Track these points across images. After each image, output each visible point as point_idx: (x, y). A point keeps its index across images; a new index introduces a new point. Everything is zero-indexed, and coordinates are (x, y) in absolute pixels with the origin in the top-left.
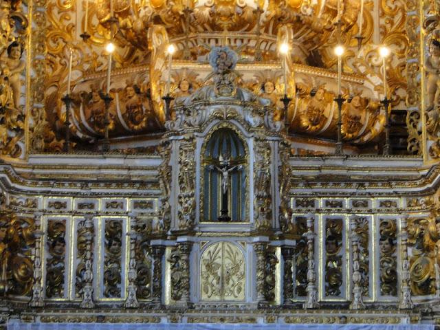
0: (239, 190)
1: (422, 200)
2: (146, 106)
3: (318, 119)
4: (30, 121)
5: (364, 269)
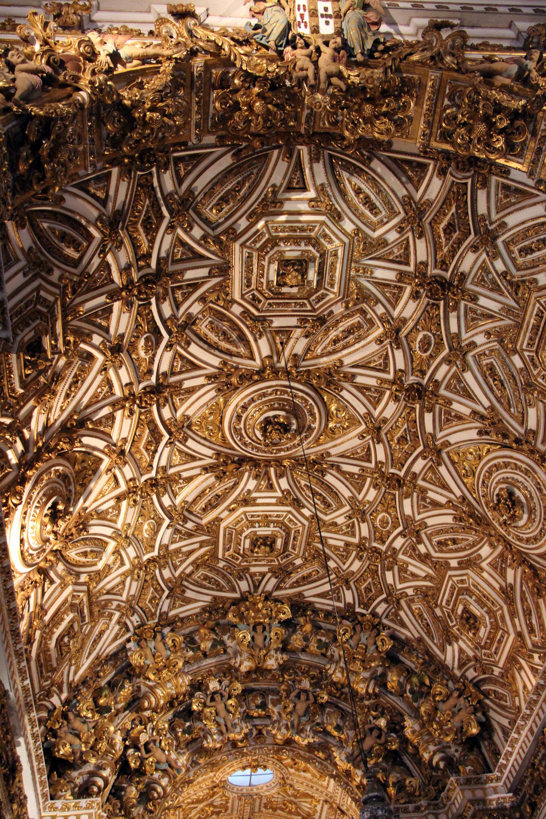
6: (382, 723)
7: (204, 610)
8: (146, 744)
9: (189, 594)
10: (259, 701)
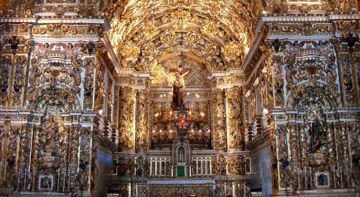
0: (184, 156)
1: (214, 158)
2: (167, 139)
3: (197, 140)
4: (149, 144)
5: (204, 169)
8: (147, 50)
9: (159, 9)
10: (181, 36)
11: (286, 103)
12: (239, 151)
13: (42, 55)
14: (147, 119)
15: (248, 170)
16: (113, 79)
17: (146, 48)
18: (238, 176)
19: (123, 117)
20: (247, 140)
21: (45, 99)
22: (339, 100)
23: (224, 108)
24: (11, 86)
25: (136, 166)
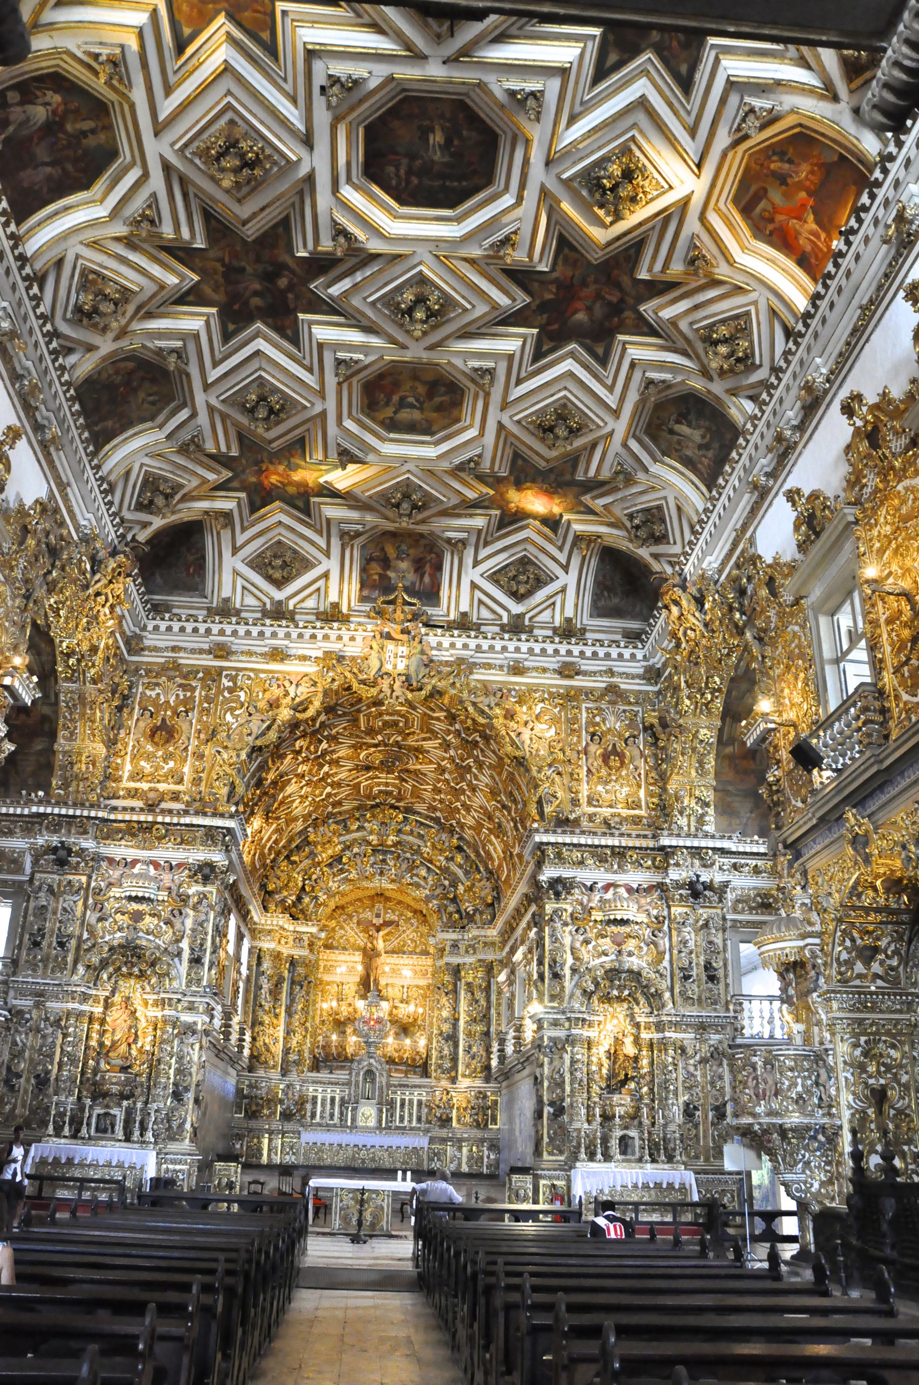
3: (401, 1058)
5: (411, 1115)
6: (446, 883)
7: (353, 809)
11: (567, 998)
12: (478, 1083)
13: (112, 881)
14: (307, 1013)
15: (494, 1121)
16: (246, 933)
17: (314, 877)
18: (476, 1131)
19: (261, 1006)
20: (494, 1063)
21: (113, 963)
22: (667, 995)
23: (456, 1000)
24: (51, 936)
25: (281, 1102)
